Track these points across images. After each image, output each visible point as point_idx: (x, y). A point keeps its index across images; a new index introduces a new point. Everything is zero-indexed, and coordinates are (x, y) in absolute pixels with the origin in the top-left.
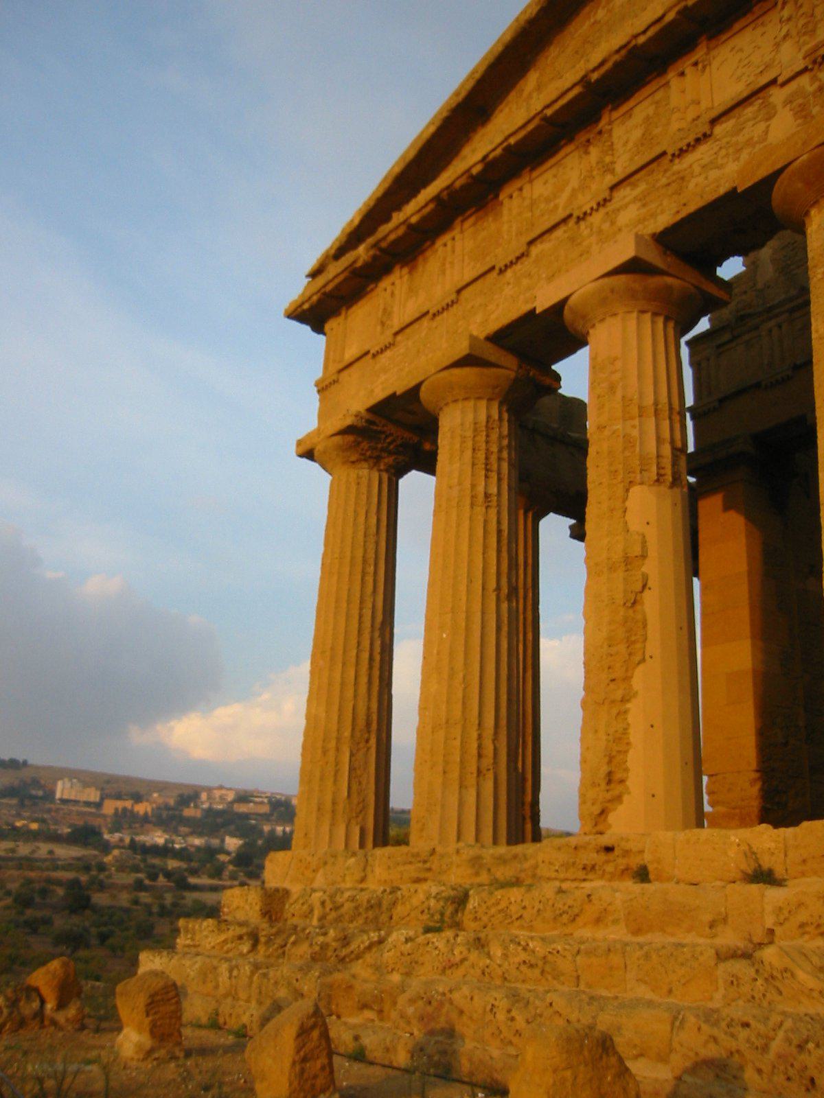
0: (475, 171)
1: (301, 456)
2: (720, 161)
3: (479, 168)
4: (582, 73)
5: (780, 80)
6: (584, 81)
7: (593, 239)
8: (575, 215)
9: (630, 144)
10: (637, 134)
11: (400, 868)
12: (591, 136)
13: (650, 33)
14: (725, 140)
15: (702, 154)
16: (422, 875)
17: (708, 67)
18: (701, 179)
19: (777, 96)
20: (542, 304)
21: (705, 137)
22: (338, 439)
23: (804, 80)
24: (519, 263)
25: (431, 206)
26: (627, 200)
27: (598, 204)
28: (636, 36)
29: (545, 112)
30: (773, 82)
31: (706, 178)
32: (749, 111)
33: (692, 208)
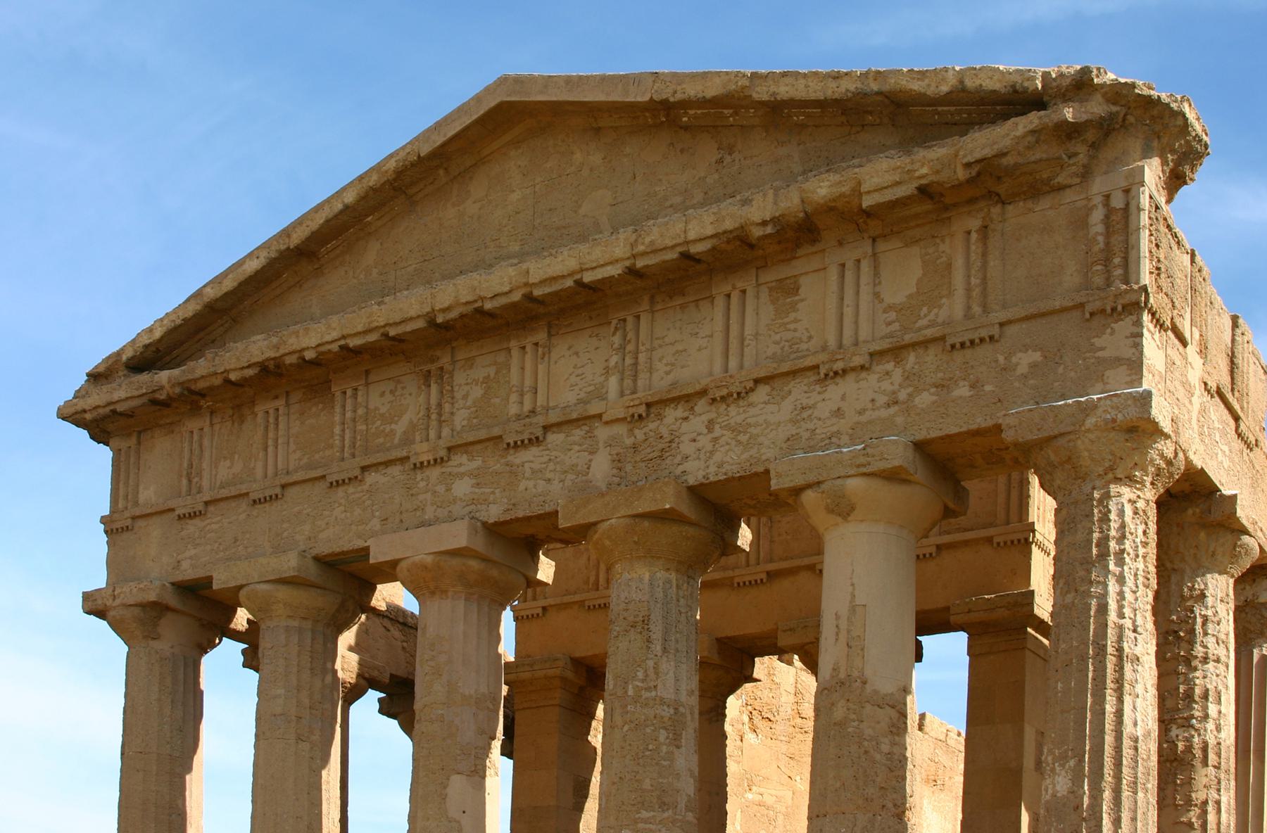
1: (89, 613)
2: (549, 475)
4: (428, 309)
7: (429, 496)
8: (413, 460)
10: (477, 392)
12: (433, 367)
14: (554, 453)
15: (534, 456)
17: (547, 355)
18: (531, 484)
19: (602, 433)
21: (536, 441)
22: (137, 611)
23: (621, 429)
24: (351, 486)
26: (462, 469)
27: (435, 460)
29: (387, 328)
30: (599, 416)
31: (535, 486)
32: (578, 433)
33: (521, 514)
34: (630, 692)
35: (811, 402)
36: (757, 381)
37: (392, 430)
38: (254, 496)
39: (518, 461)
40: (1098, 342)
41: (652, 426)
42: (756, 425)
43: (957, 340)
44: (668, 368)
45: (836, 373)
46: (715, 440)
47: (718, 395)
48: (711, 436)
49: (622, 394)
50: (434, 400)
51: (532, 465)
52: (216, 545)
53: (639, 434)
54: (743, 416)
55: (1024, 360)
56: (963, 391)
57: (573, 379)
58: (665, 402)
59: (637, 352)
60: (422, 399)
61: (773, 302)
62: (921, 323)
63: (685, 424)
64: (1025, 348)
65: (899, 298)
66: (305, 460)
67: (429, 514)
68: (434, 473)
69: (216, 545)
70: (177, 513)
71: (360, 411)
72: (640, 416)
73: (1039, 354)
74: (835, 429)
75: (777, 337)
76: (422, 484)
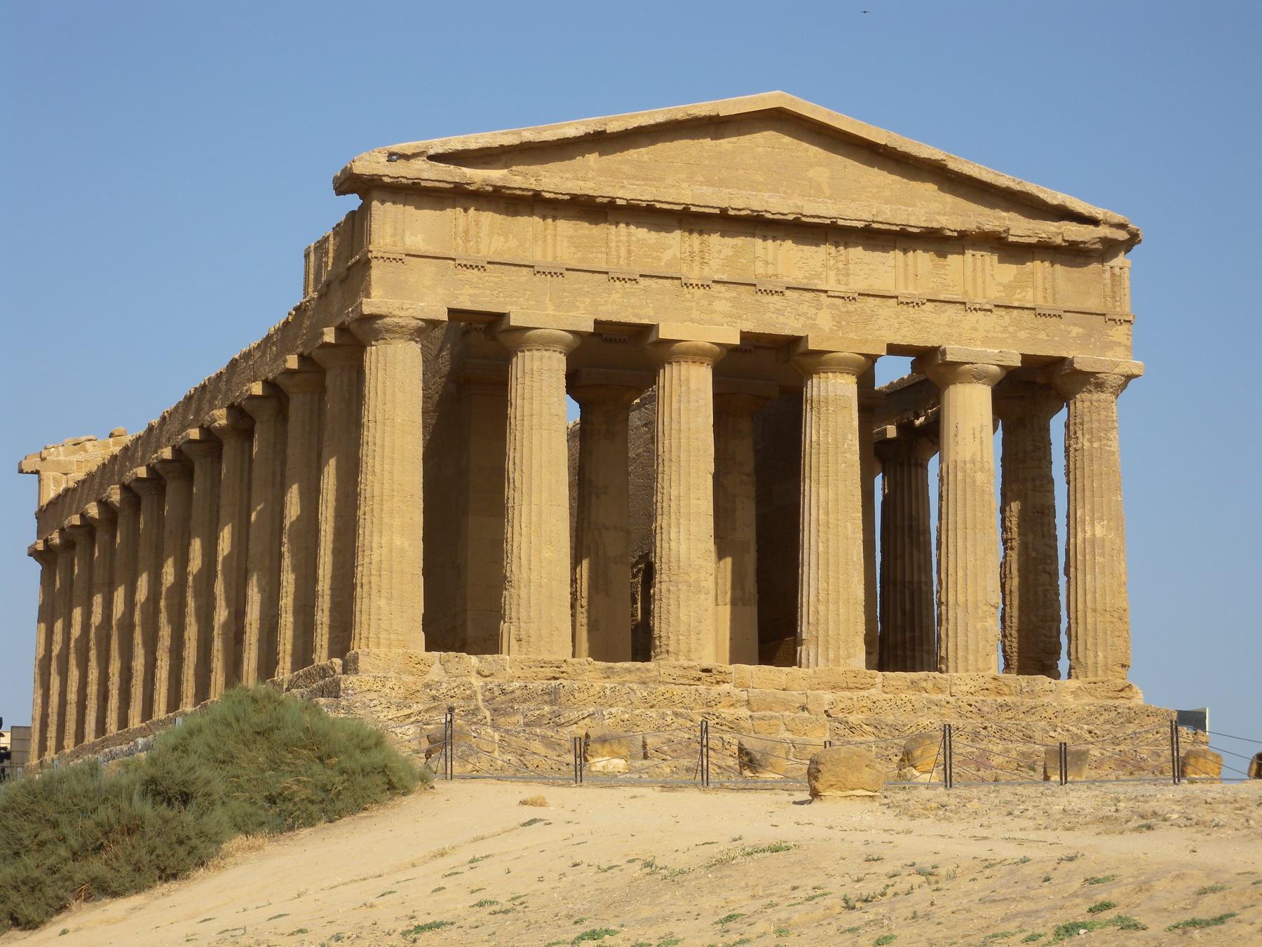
0: (619, 202)
3: (624, 203)
5: (830, 293)
6: (724, 211)
7: (694, 304)
9: (722, 256)
10: (728, 252)
11: (532, 670)
13: (776, 217)
16: (557, 676)
18: (774, 316)
20: (664, 334)
22: (421, 323)
25: (567, 197)
26: (721, 295)
28: (766, 211)
30: (826, 292)
34: (846, 446)
35: (958, 318)
36: (928, 300)
37: (658, 256)
38: (537, 269)
39: (764, 301)
40: (1110, 333)
41: (858, 304)
42: (926, 322)
43: (1043, 312)
44: (866, 276)
45: (975, 309)
46: (900, 323)
47: (905, 300)
48: (897, 320)
49: (839, 282)
50: (696, 248)
51: (776, 306)
52: (495, 292)
53: (851, 307)
54: (918, 316)
55: (1076, 331)
56: (1042, 336)
57: (800, 264)
58: (869, 295)
59: (847, 263)
60: (686, 245)
61: (932, 261)
62: (1017, 296)
63: (880, 310)
64: (1075, 325)
65: (1005, 281)
66: (579, 255)
67: (695, 314)
68: (699, 292)
69: (495, 292)
70: (458, 262)
71: (634, 239)
72: (854, 299)
73: (1081, 330)
74: (973, 336)
75: (935, 280)
76: (688, 296)
